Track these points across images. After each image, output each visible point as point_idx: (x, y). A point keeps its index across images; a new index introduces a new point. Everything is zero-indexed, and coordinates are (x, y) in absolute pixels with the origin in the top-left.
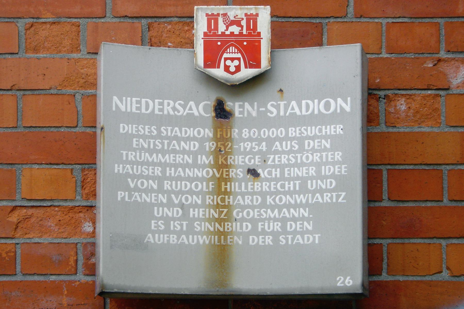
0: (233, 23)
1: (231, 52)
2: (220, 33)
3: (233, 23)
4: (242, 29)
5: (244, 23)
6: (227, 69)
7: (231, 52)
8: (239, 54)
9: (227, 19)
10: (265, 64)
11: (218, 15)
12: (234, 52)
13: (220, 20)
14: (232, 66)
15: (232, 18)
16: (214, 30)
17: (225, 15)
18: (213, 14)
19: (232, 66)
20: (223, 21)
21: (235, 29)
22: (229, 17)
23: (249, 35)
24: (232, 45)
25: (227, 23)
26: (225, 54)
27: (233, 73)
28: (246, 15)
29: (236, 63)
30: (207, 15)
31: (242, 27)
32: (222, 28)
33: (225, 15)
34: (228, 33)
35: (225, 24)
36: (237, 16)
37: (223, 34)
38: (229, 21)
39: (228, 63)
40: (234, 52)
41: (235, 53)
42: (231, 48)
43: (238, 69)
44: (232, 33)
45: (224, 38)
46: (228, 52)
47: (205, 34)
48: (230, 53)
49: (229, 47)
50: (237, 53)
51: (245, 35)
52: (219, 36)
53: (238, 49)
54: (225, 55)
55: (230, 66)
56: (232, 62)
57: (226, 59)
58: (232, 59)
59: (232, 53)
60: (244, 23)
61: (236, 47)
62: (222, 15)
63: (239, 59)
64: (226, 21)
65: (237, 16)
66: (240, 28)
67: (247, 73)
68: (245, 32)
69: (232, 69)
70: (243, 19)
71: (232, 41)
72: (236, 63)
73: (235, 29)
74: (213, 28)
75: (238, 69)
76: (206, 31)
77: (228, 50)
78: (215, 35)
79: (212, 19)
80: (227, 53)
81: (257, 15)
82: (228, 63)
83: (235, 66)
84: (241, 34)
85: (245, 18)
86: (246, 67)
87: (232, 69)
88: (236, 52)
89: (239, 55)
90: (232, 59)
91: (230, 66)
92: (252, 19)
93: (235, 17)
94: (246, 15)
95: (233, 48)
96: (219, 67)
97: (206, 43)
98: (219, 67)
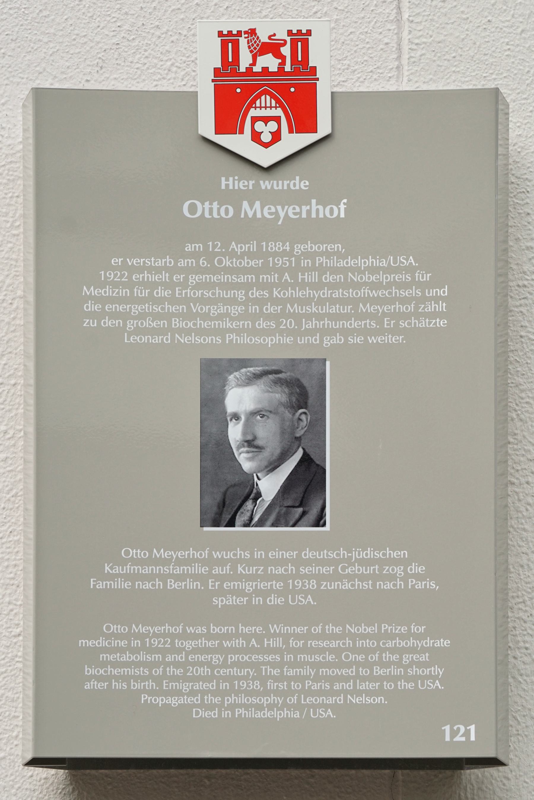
1: (263, 105)
2: (243, 69)
4: (283, 63)
5: (286, 51)
6: (256, 137)
7: (263, 105)
8: (279, 109)
9: (255, 42)
10: (324, 127)
11: (239, 33)
12: (268, 105)
13: (243, 42)
14: (266, 131)
15: (264, 39)
17: (252, 32)
19: (266, 131)
20: (249, 47)
21: (269, 62)
22: (258, 38)
23: (295, 72)
24: (266, 92)
25: (255, 48)
26: (252, 110)
27: (267, 145)
28: (290, 33)
29: (273, 126)
30: (220, 34)
31: (283, 58)
32: (245, 59)
33: (252, 32)
34: (257, 69)
35: (251, 52)
36: (274, 35)
37: (249, 70)
38: (258, 45)
39: (259, 126)
40: (268, 105)
41: (271, 107)
42: (263, 97)
43: (276, 137)
45: (250, 81)
46: (258, 104)
47: (216, 70)
48: (261, 107)
49: (259, 97)
50: (276, 107)
53: (278, 101)
54: (253, 112)
57: (255, 120)
58: (266, 120)
59: (266, 107)
60: (286, 51)
61: (272, 96)
62: (246, 32)
63: (277, 119)
64: (253, 45)
66: (280, 61)
67: (293, 142)
68: (288, 68)
69: (266, 138)
72: (273, 126)
73: (269, 62)
74: (230, 60)
75: (276, 137)
76: (219, 66)
77: (258, 102)
78: (235, 73)
80: (256, 108)
81: (309, 33)
82: (259, 126)
84: (281, 69)
85: (288, 39)
86: (291, 131)
87: (266, 138)
88: (273, 104)
89: (279, 112)
90: (266, 120)
93: (270, 38)
94: (290, 33)
95: (268, 97)
96: (242, 132)
97: (218, 89)
98: (242, 132)
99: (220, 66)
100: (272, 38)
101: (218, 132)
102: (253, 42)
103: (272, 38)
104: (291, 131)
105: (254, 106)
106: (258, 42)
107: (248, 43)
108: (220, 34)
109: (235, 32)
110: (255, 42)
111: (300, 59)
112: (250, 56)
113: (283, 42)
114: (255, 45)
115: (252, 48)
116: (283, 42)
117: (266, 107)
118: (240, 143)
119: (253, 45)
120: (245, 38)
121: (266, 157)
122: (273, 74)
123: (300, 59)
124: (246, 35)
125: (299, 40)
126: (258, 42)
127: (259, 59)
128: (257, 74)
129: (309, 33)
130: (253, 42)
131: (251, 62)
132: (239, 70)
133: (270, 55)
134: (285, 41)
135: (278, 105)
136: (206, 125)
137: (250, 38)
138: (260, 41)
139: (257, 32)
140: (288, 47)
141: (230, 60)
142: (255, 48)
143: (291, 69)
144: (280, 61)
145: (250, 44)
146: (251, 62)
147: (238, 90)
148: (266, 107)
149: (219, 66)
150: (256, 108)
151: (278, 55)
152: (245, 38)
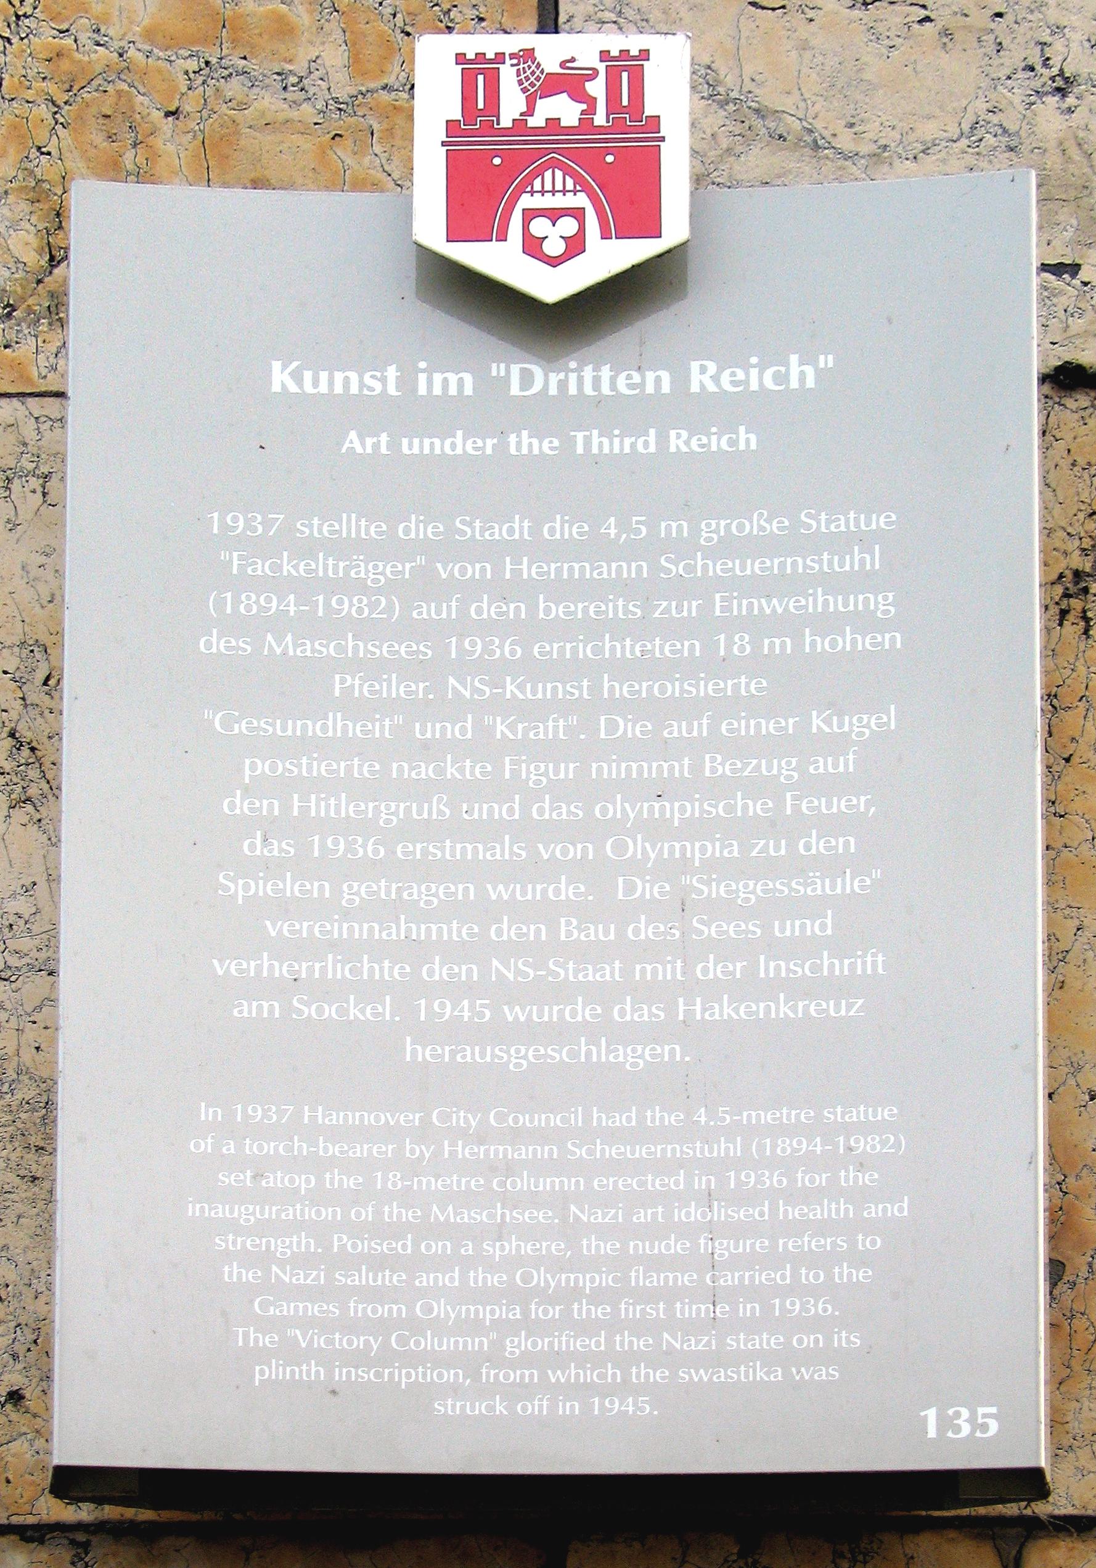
0: (553, 85)
1: (548, 186)
2: (506, 122)
3: (553, 85)
4: (592, 109)
5: (597, 88)
6: (533, 247)
7: (548, 186)
9: (533, 73)
10: (675, 227)
11: (500, 58)
12: (559, 186)
13: (508, 74)
15: (551, 66)
17: (528, 55)
20: (520, 83)
21: (563, 109)
23: (617, 126)
24: (554, 165)
25: (532, 85)
27: (554, 262)
28: (604, 55)
29: (568, 226)
30: (460, 58)
31: (592, 102)
33: (528, 55)
34: (536, 121)
35: (524, 90)
36: (573, 60)
37: (519, 124)
39: (540, 226)
40: (559, 186)
41: (564, 192)
42: (548, 174)
43: (575, 246)
44: (553, 124)
47: (452, 126)
48: (543, 192)
49: (539, 173)
50: (575, 192)
51: (601, 130)
52: (505, 132)
53: (578, 179)
54: (527, 201)
57: (529, 215)
58: (554, 215)
59: (553, 192)
60: (597, 88)
61: (567, 172)
62: (512, 56)
63: (578, 214)
66: (584, 106)
67: (608, 257)
68: (600, 119)
69: (554, 247)
71: (554, 150)
72: (568, 226)
73: (563, 109)
74: (481, 105)
76: (457, 115)
78: (490, 128)
79: (478, 73)
80: (532, 193)
81: (645, 54)
82: (540, 226)
84: (586, 122)
85: (602, 67)
86: (605, 235)
87: (554, 247)
88: (570, 184)
89: (581, 200)
90: (554, 215)
92: (627, 69)
93: (563, 65)
94: (604, 55)
95: (559, 174)
96: (503, 237)
97: (452, 159)
98: (503, 237)
99: (460, 117)
100: (568, 65)
101: (452, 237)
102: (528, 73)
103: (568, 65)
104: (605, 235)
105: (529, 189)
106: (538, 73)
107: (518, 74)
108: (460, 58)
109: (490, 55)
110: (533, 73)
111: (625, 102)
112: (523, 97)
113: (590, 72)
114: (532, 79)
115: (526, 84)
116: (590, 72)
117: (555, 190)
118: (499, 260)
119: (527, 78)
120: (512, 65)
121: (551, 286)
122: (569, 130)
123: (625, 102)
124: (515, 61)
125: (625, 68)
126: (538, 73)
127: (541, 104)
128: (536, 130)
129: (645, 54)
130: (528, 73)
131: (525, 109)
132: (498, 124)
133: (565, 94)
134: (596, 72)
135: (578, 188)
136: (430, 226)
137: (521, 66)
138: (542, 72)
139: (536, 54)
141: (481, 105)
142: (532, 85)
143: (608, 122)
144: (584, 106)
145: (522, 77)
146: (525, 109)
147: (497, 161)
148: (555, 190)
149: (457, 115)
150: (532, 193)
151: (578, 94)
152: (512, 65)
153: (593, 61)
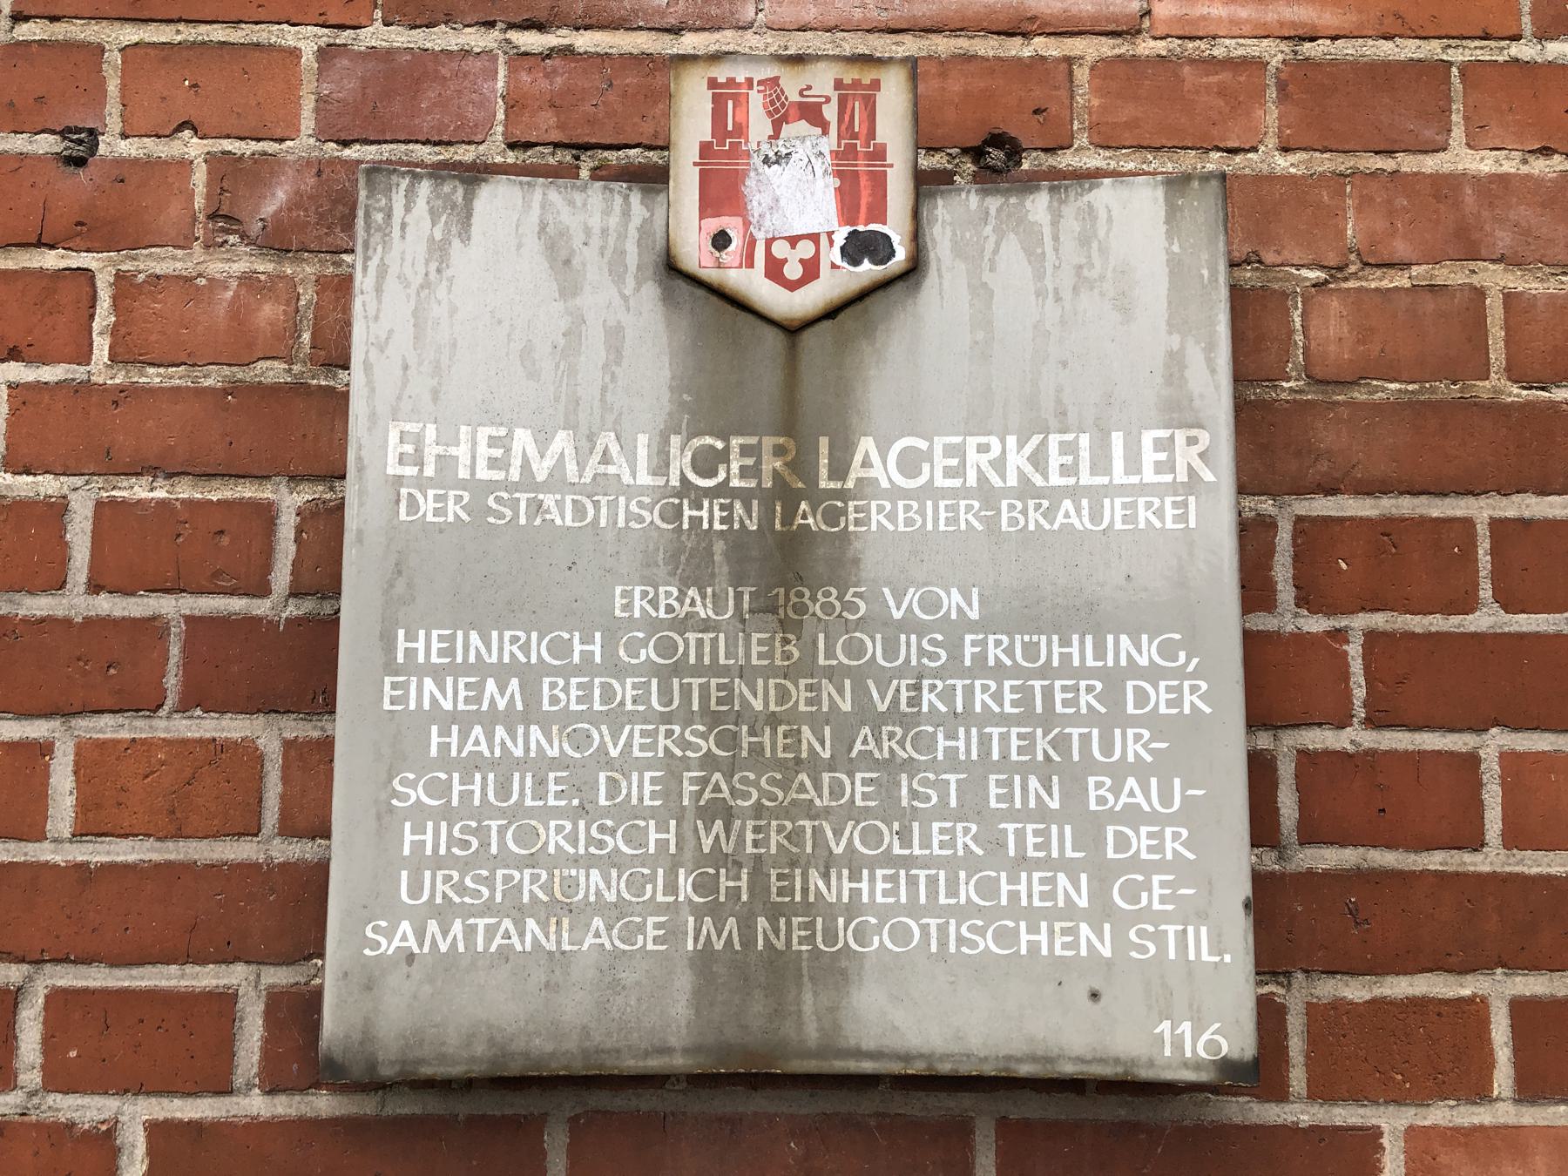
5: (830, 113)
6: (774, 270)
9: (778, 98)
13: (756, 100)
16: (730, 135)
18: (731, 82)
27: (792, 286)
28: (839, 84)
30: (713, 83)
35: (770, 114)
43: (811, 270)
47: (705, 149)
55: (785, 261)
56: (793, 246)
60: (830, 113)
62: (760, 83)
65: (809, 88)
69: (793, 271)
70: (828, 100)
75: (811, 270)
81: (876, 85)
82: (780, 250)
83: (801, 261)
87: (793, 271)
91: (785, 261)
93: (801, 94)
97: (705, 177)
140: (835, 101)
142: (777, 111)
153: (828, 90)
